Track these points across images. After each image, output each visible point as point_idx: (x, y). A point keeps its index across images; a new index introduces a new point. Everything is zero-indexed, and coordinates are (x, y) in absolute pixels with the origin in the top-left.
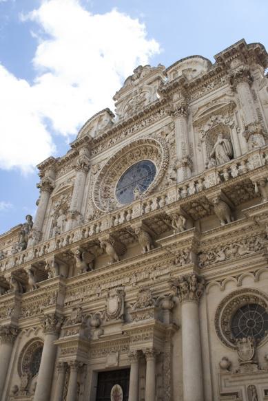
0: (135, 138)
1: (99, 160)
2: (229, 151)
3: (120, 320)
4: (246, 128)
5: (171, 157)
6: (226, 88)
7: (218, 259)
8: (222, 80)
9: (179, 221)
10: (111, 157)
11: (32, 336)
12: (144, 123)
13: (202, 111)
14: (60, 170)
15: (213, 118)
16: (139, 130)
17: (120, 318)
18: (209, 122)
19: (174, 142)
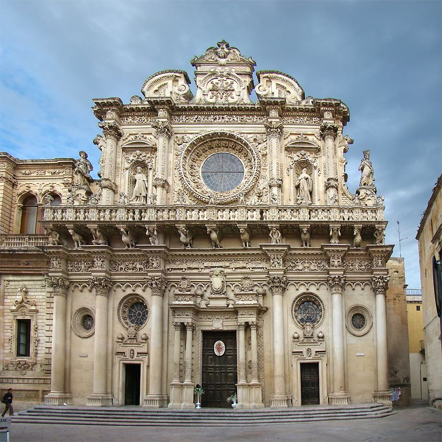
0: (227, 129)
1: (182, 130)
2: (310, 188)
3: (223, 296)
4: (328, 180)
5: (262, 167)
6: (316, 130)
7: (297, 268)
8: (314, 120)
9: (276, 233)
10: (199, 136)
11: (129, 291)
12: (235, 119)
13: (294, 137)
14: (127, 116)
15: (303, 152)
16: (227, 123)
17: (224, 294)
18: (298, 153)
19: (266, 154)
